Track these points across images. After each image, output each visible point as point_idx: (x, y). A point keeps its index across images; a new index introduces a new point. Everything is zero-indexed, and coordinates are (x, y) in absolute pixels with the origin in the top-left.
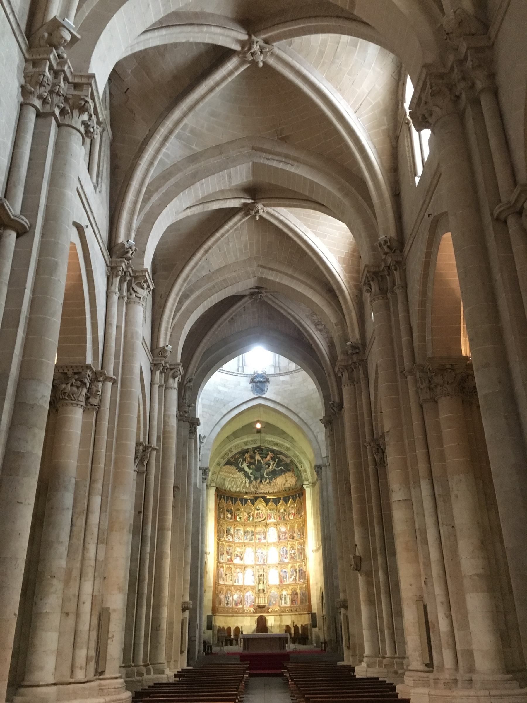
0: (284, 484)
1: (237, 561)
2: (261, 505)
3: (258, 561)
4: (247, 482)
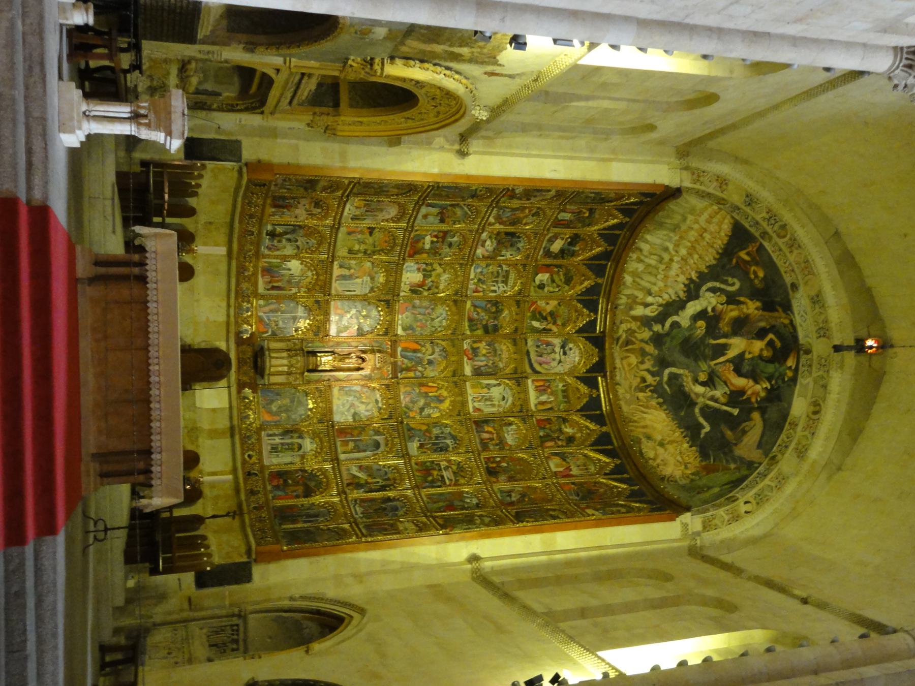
1: (411, 275)
3: (405, 349)
4: (649, 312)
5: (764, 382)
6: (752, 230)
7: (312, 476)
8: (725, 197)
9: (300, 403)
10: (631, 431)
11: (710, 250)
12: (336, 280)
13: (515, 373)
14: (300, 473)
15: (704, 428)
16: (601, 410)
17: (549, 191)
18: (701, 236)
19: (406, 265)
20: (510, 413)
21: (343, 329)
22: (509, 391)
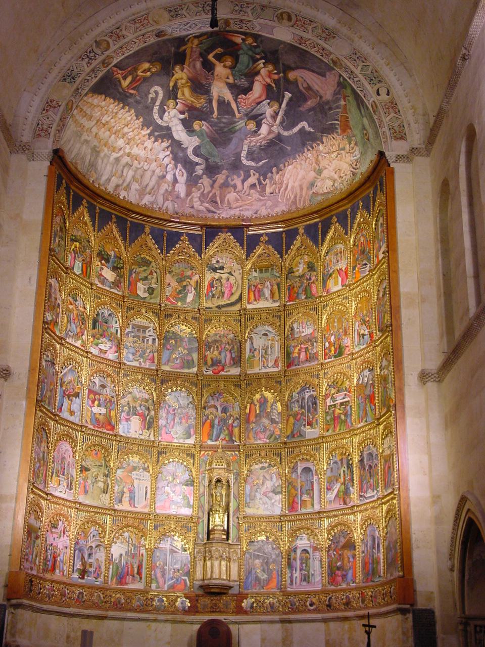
0: (312, 185)
1: (131, 428)
2: (225, 254)
3: (210, 437)
4: (182, 179)
5: (257, 66)
6: (100, 75)
7: (334, 541)
8: (64, 104)
9: (259, 550)
10: (304, 202)
11: (120, 116)
12: (134, 507)
13: (241, 321)
14: (331, 552)
15: (304, 127)
16: (282, 232)
17: (51, 285)
18: (104, 125)
19: (121, 433)
20: (281, 328)
21: (186, 501)
22: (258, 329)
